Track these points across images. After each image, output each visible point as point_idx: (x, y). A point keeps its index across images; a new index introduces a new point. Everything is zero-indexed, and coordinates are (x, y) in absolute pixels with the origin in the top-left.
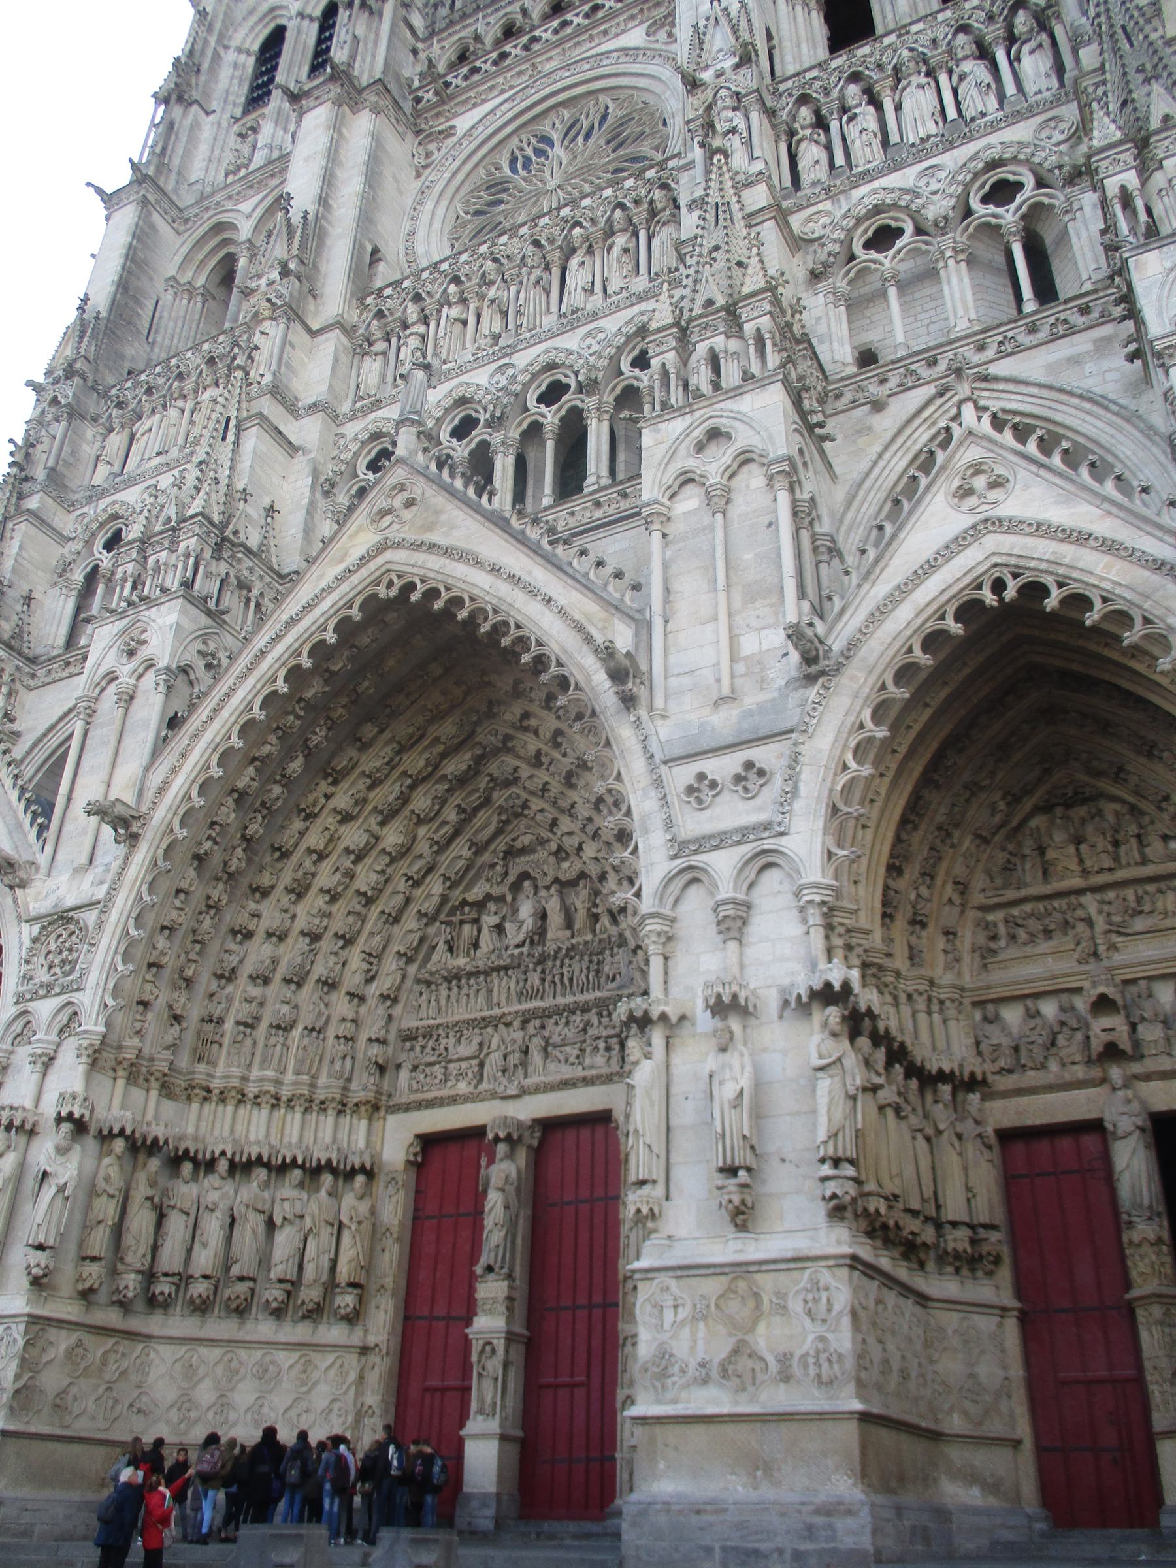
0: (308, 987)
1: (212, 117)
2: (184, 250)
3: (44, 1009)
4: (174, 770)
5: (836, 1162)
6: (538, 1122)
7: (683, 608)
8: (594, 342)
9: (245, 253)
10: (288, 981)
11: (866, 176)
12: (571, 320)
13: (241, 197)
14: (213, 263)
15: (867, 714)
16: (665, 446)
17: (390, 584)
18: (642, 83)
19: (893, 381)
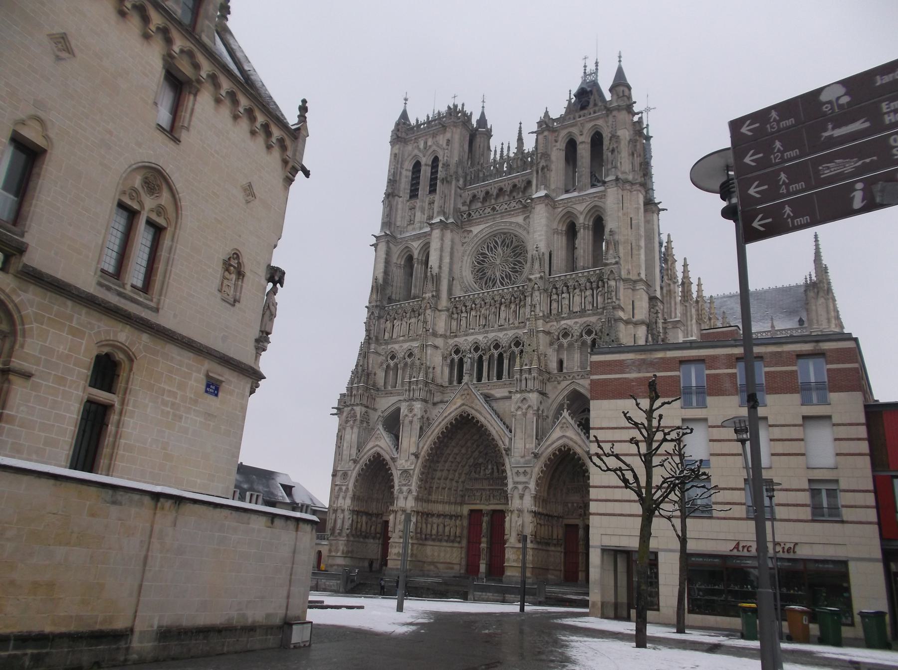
0: (448, 480)
1: (401, 199)
2: (398, 253)
3: (405, 489)
4: (425, 444)
6: (492, 510)
7: (517, 435)
9: (416, 262)
10: (444, 479)
11: (563, 319)
12: (501, 328)
13: (413, 240)
14: (405, 257)
19: (562, 378)
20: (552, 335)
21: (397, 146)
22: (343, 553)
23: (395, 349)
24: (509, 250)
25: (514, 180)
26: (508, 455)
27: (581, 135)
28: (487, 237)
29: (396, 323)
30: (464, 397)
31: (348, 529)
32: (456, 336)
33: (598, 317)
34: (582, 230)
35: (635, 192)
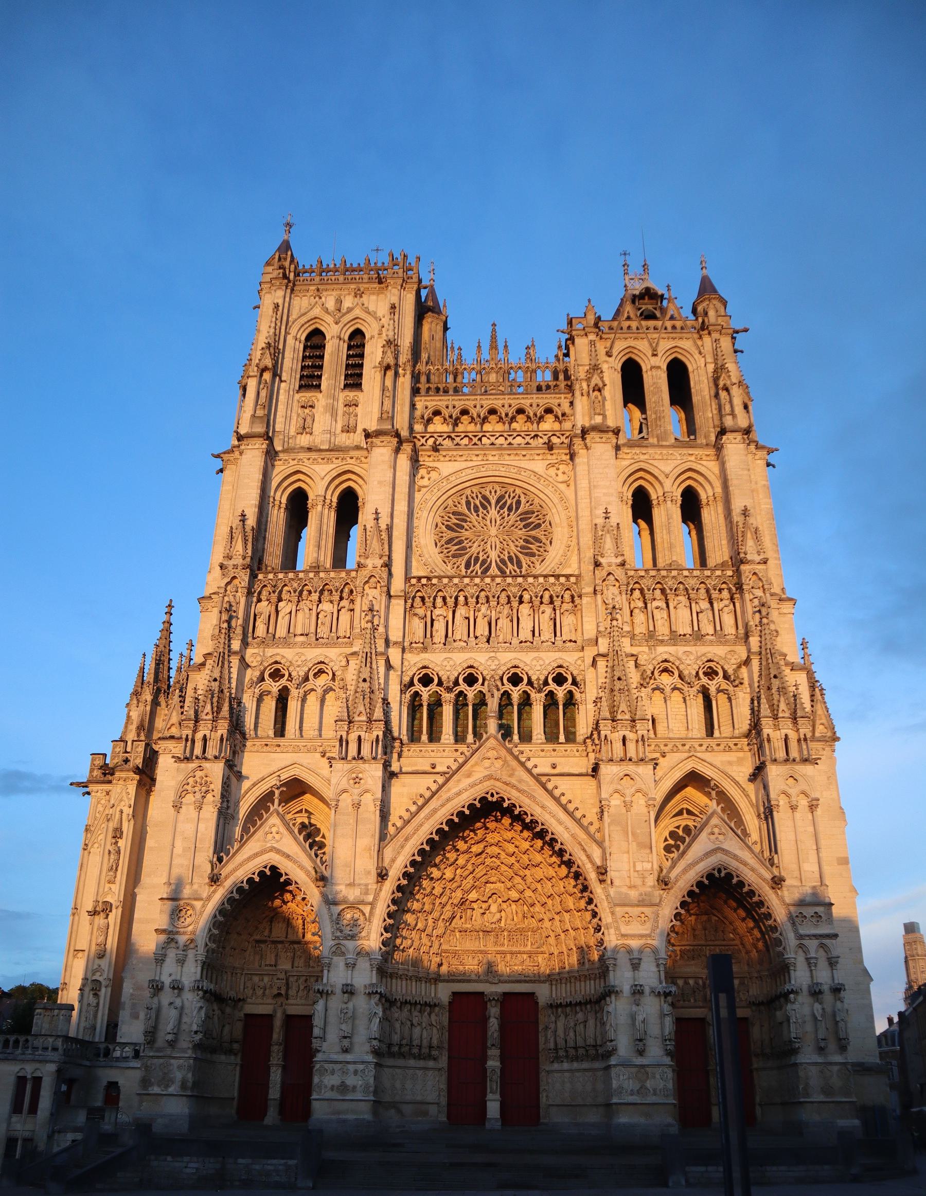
1: (283, 385)
5: (670, 1040)
8: (538, 664)
15: (678, 905)
16: (610, 776)
17: (492, 795)
18: (541, 495)
19: (670, 747)
20: (642, 668)
21: (280, 293)
22: (183, 1086)
23: (283, 657)
24: (513, 517)
25: (522, 401)
26: (602, 881)
27: (655, 355)
28: (468, 484)
29: (284, 607)
30: (487, 763)
31: (196, 1032)
32: (425, 649)
33: (728, 648)
34: (669, 503)
35: (759, 462)
